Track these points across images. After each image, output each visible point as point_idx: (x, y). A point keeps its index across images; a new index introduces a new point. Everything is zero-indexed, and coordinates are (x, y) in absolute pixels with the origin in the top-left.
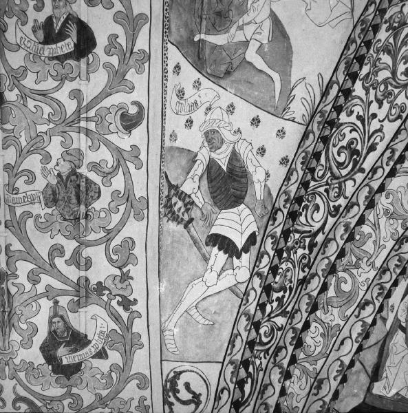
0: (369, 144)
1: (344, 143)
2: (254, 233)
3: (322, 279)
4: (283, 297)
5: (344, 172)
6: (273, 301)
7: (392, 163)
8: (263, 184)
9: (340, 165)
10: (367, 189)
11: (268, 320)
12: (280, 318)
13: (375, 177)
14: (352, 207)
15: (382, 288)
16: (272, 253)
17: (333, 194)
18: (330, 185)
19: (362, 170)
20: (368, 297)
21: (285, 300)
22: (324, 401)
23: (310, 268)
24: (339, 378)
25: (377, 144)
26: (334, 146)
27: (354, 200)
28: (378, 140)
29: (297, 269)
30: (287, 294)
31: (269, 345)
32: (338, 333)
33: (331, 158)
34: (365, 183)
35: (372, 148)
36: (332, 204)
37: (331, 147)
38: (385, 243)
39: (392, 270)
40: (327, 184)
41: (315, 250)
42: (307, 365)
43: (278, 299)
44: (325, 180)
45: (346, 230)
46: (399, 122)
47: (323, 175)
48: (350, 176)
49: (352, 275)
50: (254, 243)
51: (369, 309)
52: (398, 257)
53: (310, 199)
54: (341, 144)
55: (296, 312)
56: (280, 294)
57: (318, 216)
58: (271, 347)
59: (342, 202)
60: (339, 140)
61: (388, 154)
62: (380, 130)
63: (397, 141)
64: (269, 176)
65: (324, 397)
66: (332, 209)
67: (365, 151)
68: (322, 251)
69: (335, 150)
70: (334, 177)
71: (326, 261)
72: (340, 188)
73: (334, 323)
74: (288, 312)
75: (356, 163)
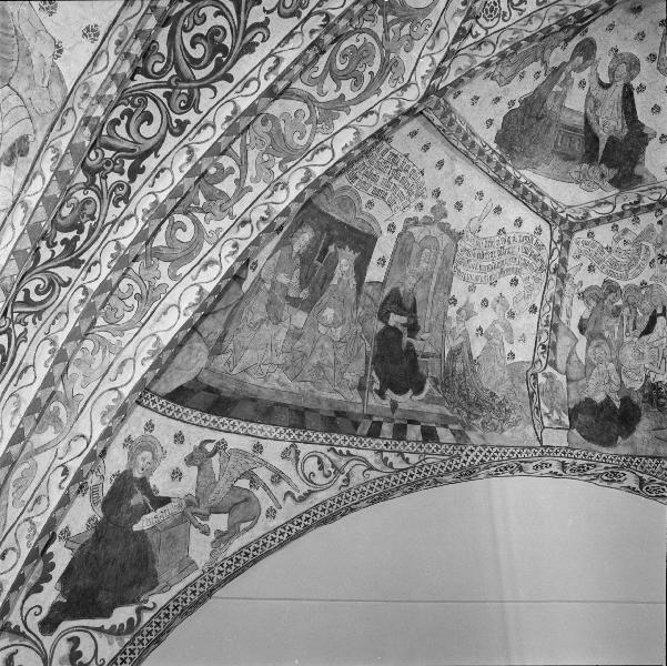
0: (245, 42)
1: (203, 29)
2: (24, 139)
3: (141, 223)
4: (76, 239)
5: (200, 74)
6: (55, 244)
7: (272, 78)
8: (49, 61)
9: (194, 63)
10: (230, 107)
11: (44, 271)
12: (67, 268)
13: (245, 92)
14: (205, 126)
15: (236, 245)
16: (48, 175)
17: (180, 101)
18: (174, 88)
19: (229, 78)
20: (214, 255)
21: (79, 244)
22: (120, 393)
23: (127, 202)
24: (151, 362)
25: (257, 44)
26: (185, 29)
27: (210, 118)
28: (258, 38)
29: (106, 201)
30: (83, 236)
31: (44, 306)
32: (162, 296)
33: (178, 47)
34: (228, 98)
35: (249, 48)
36: (174, 117)
37: (179, 29)
38: (252, 185)
39: (254, 223)
40: (169, 84)
41: (140, 178)
42: (107, 336)
43: (64, 241)
44: (166, 79)
45: (189, 160)
46: (294, 21)
47: (163, 72)
48: (208, 83)
49: (196, 222)
50: (24, 153)
51: (213, 271)
52: (265, 208)
53: (136, 102)
54: (197, 30)
55: (95, 263)
56: (70, 235)
57: (147, 131)
58: (45, 309)
59: (192, 116)
60: (195, 23)
61: (270, 62)
62: (264, 24)
63: (286, 47)
64: (61, 51)
65: (122, 386)
66: (175, 125)
67: (236, 51)
68: (150, 182)
69: (187, 38)
70: (181, 77)
71: (152, 199)
72: (190, 96)
73: (159, 282)
74: (83, 261)
75: (217, 68)
